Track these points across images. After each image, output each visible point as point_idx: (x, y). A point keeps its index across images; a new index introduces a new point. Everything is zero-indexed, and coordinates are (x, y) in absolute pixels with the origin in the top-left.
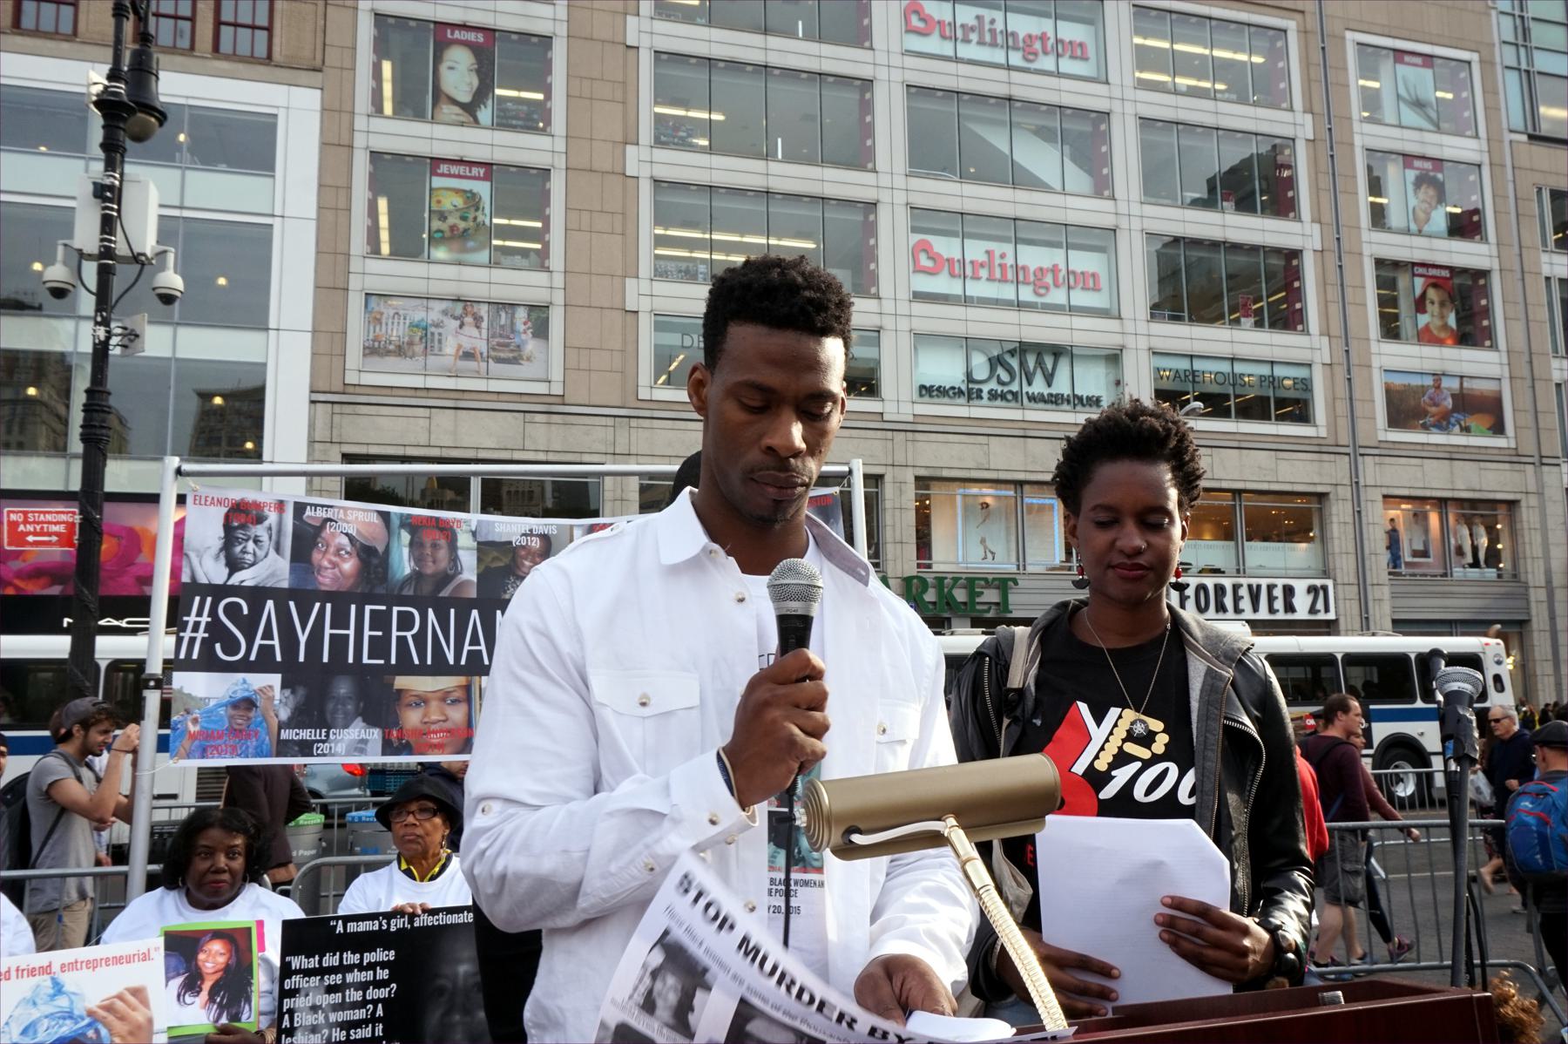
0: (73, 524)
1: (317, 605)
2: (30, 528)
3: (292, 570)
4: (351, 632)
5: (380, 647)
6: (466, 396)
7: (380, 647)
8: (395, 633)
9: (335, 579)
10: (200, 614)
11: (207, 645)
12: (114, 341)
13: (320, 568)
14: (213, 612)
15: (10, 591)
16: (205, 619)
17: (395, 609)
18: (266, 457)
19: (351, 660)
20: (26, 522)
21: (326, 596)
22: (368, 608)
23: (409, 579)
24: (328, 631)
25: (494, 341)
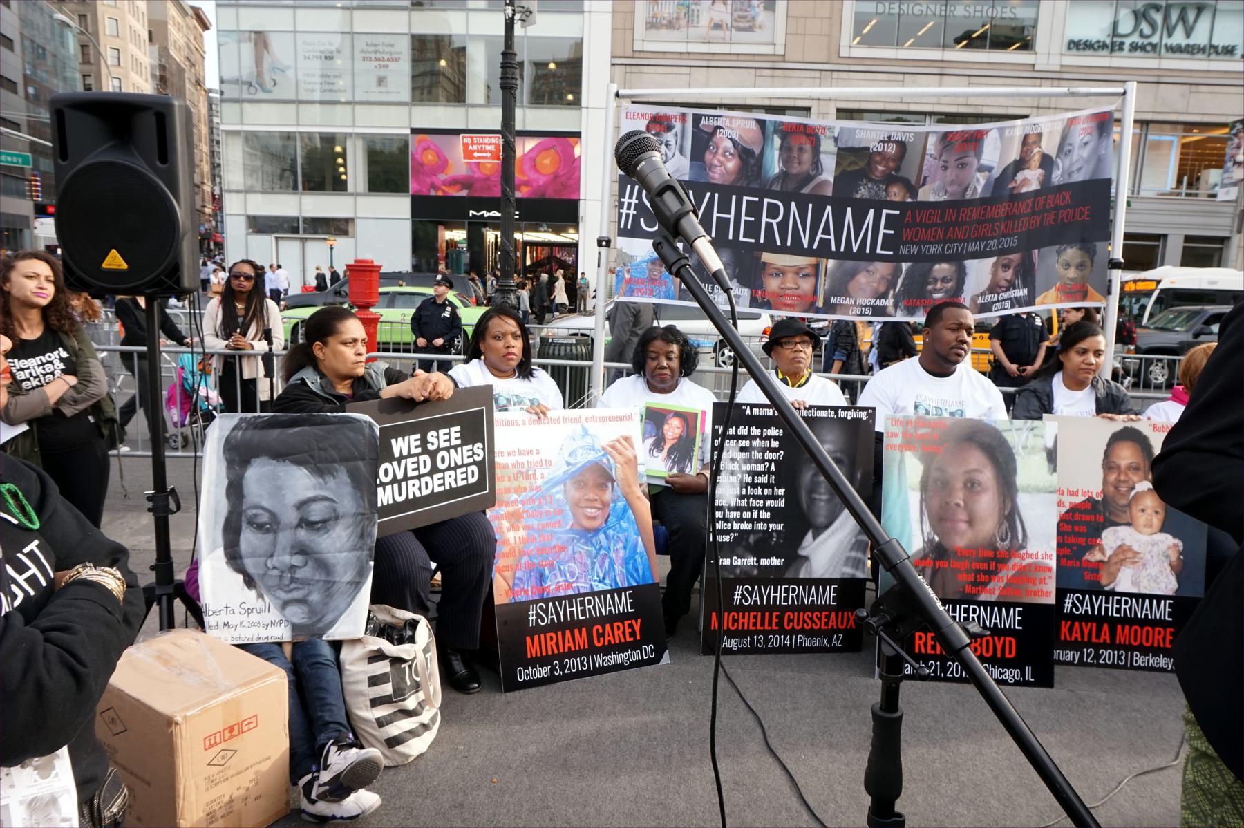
0: (497, 146)
1: (708, 194)
2: (475, 147)
3: (691, 167)
4: (732, 216)
5: (752, 229)
6: (716, 57)
7: (752, 229)
8: (764, 220)
9: (722, 175)
10: (631, 197)
11: (636, 219)
12: (517, 17)
13: (712, 166)
14: (639, 197)
15: (440, 193)
16: (634, 201)
17: (766, 201)
18: (584, 104)
19: (730, 237)
20: (473, 143)
21: (714, 188)
22: (745, 198)
23: (778, 177)
24: (716, 215)
25: (736, 14)
